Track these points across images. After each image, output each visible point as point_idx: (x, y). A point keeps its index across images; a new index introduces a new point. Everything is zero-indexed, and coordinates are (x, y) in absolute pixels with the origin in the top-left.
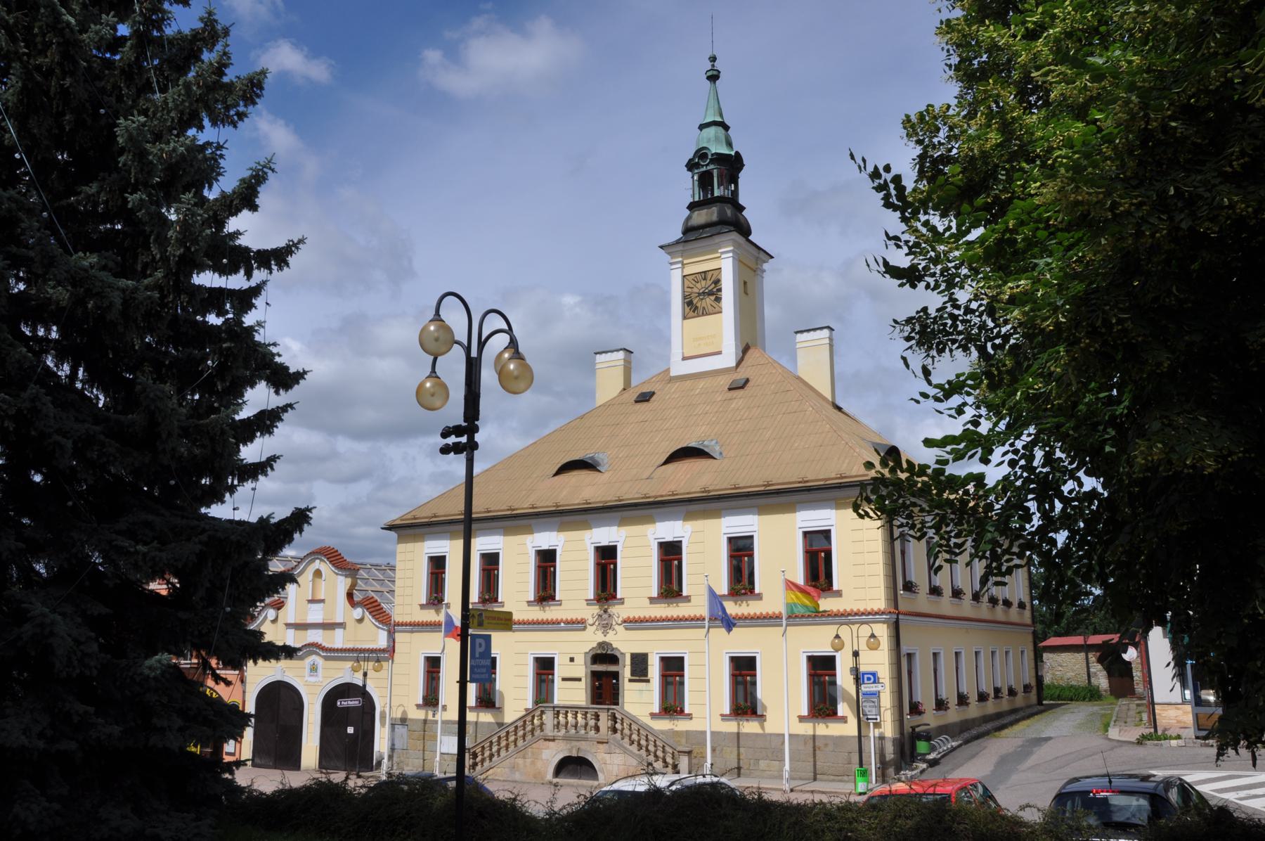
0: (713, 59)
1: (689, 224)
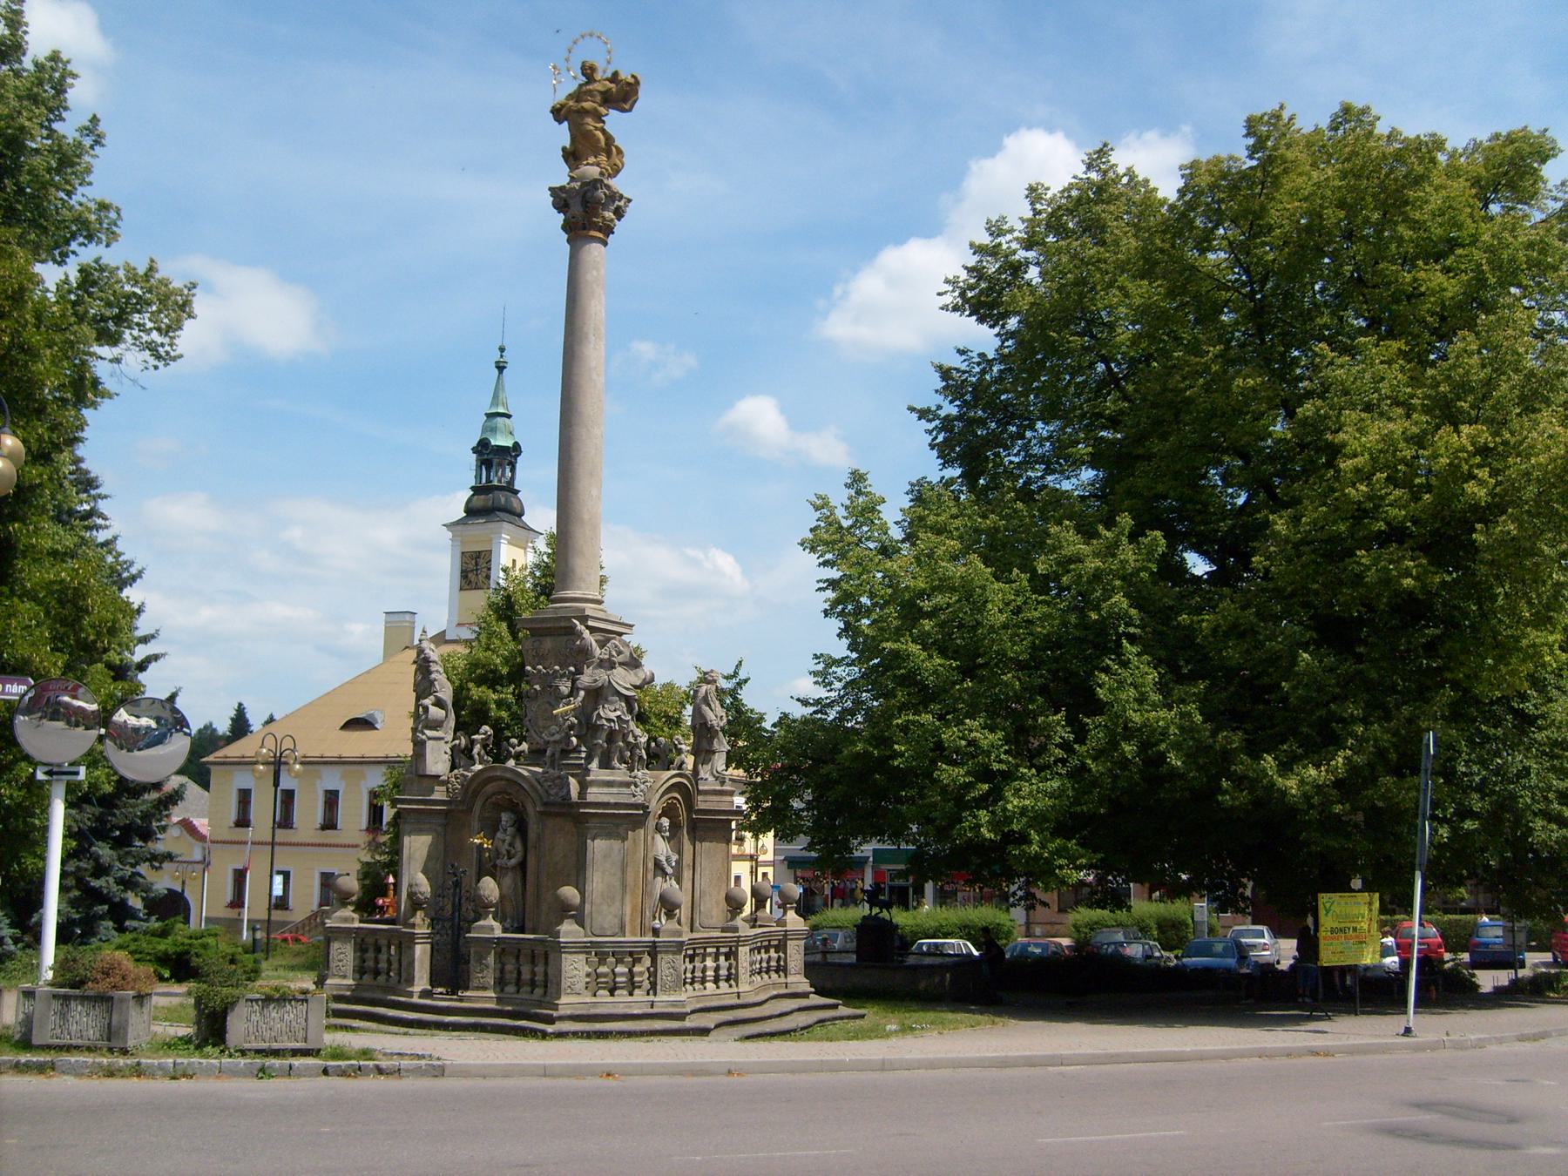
0: (502, 350)
1: (470, 505)
